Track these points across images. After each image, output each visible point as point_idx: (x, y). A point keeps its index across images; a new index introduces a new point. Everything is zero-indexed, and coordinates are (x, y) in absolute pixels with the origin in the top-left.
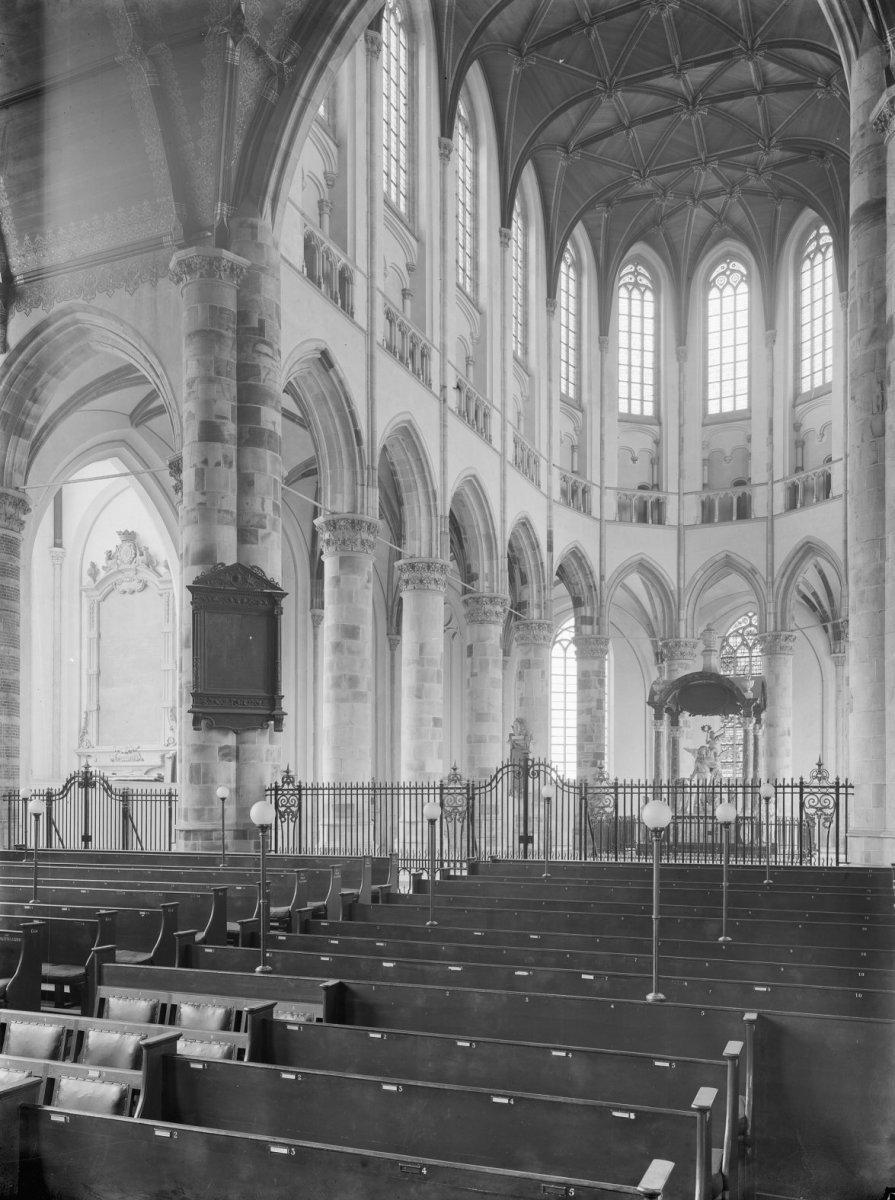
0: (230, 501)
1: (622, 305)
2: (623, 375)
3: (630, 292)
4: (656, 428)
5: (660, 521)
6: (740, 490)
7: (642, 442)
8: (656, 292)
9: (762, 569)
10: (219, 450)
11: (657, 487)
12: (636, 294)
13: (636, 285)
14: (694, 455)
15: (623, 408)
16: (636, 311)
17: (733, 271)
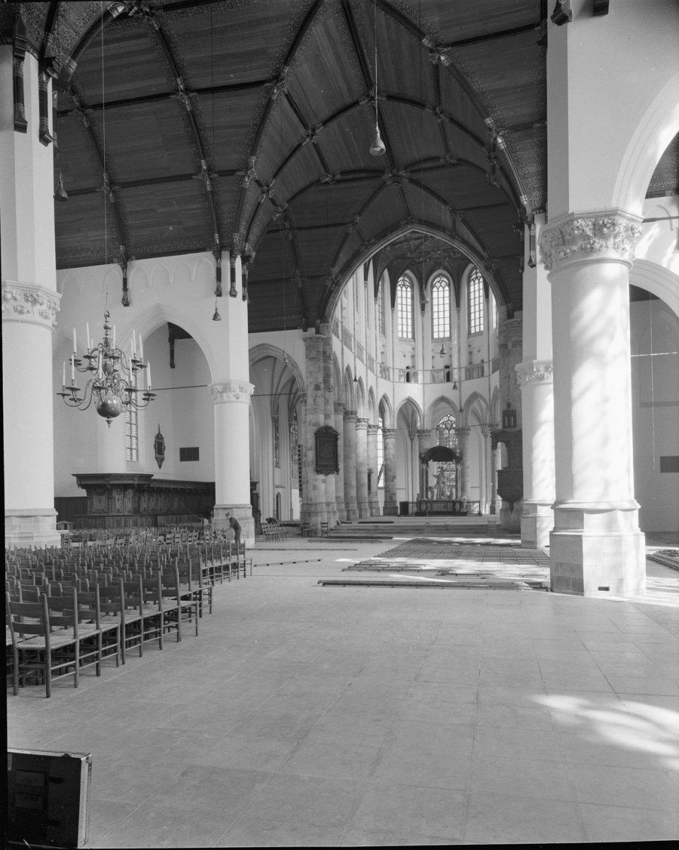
0: (322, 407)
1: (399, 293)
2: (400, 320)
3: (402, 288)
4: (413, 344)
5: (416, 381)
6: (447, 370)
7: (408, 349)
8: (412, 287)
9: (457, 403)
10: (320, 393)
11: (413, 367)
12: (404, 289)
13: (404, 285)
14: (429, 354)
15: (400, 335)
16: (404, 295)
17: (443, 281)
